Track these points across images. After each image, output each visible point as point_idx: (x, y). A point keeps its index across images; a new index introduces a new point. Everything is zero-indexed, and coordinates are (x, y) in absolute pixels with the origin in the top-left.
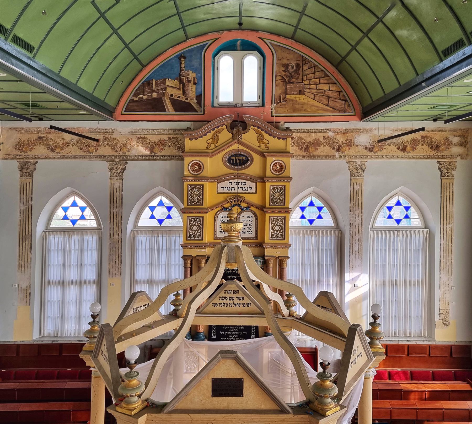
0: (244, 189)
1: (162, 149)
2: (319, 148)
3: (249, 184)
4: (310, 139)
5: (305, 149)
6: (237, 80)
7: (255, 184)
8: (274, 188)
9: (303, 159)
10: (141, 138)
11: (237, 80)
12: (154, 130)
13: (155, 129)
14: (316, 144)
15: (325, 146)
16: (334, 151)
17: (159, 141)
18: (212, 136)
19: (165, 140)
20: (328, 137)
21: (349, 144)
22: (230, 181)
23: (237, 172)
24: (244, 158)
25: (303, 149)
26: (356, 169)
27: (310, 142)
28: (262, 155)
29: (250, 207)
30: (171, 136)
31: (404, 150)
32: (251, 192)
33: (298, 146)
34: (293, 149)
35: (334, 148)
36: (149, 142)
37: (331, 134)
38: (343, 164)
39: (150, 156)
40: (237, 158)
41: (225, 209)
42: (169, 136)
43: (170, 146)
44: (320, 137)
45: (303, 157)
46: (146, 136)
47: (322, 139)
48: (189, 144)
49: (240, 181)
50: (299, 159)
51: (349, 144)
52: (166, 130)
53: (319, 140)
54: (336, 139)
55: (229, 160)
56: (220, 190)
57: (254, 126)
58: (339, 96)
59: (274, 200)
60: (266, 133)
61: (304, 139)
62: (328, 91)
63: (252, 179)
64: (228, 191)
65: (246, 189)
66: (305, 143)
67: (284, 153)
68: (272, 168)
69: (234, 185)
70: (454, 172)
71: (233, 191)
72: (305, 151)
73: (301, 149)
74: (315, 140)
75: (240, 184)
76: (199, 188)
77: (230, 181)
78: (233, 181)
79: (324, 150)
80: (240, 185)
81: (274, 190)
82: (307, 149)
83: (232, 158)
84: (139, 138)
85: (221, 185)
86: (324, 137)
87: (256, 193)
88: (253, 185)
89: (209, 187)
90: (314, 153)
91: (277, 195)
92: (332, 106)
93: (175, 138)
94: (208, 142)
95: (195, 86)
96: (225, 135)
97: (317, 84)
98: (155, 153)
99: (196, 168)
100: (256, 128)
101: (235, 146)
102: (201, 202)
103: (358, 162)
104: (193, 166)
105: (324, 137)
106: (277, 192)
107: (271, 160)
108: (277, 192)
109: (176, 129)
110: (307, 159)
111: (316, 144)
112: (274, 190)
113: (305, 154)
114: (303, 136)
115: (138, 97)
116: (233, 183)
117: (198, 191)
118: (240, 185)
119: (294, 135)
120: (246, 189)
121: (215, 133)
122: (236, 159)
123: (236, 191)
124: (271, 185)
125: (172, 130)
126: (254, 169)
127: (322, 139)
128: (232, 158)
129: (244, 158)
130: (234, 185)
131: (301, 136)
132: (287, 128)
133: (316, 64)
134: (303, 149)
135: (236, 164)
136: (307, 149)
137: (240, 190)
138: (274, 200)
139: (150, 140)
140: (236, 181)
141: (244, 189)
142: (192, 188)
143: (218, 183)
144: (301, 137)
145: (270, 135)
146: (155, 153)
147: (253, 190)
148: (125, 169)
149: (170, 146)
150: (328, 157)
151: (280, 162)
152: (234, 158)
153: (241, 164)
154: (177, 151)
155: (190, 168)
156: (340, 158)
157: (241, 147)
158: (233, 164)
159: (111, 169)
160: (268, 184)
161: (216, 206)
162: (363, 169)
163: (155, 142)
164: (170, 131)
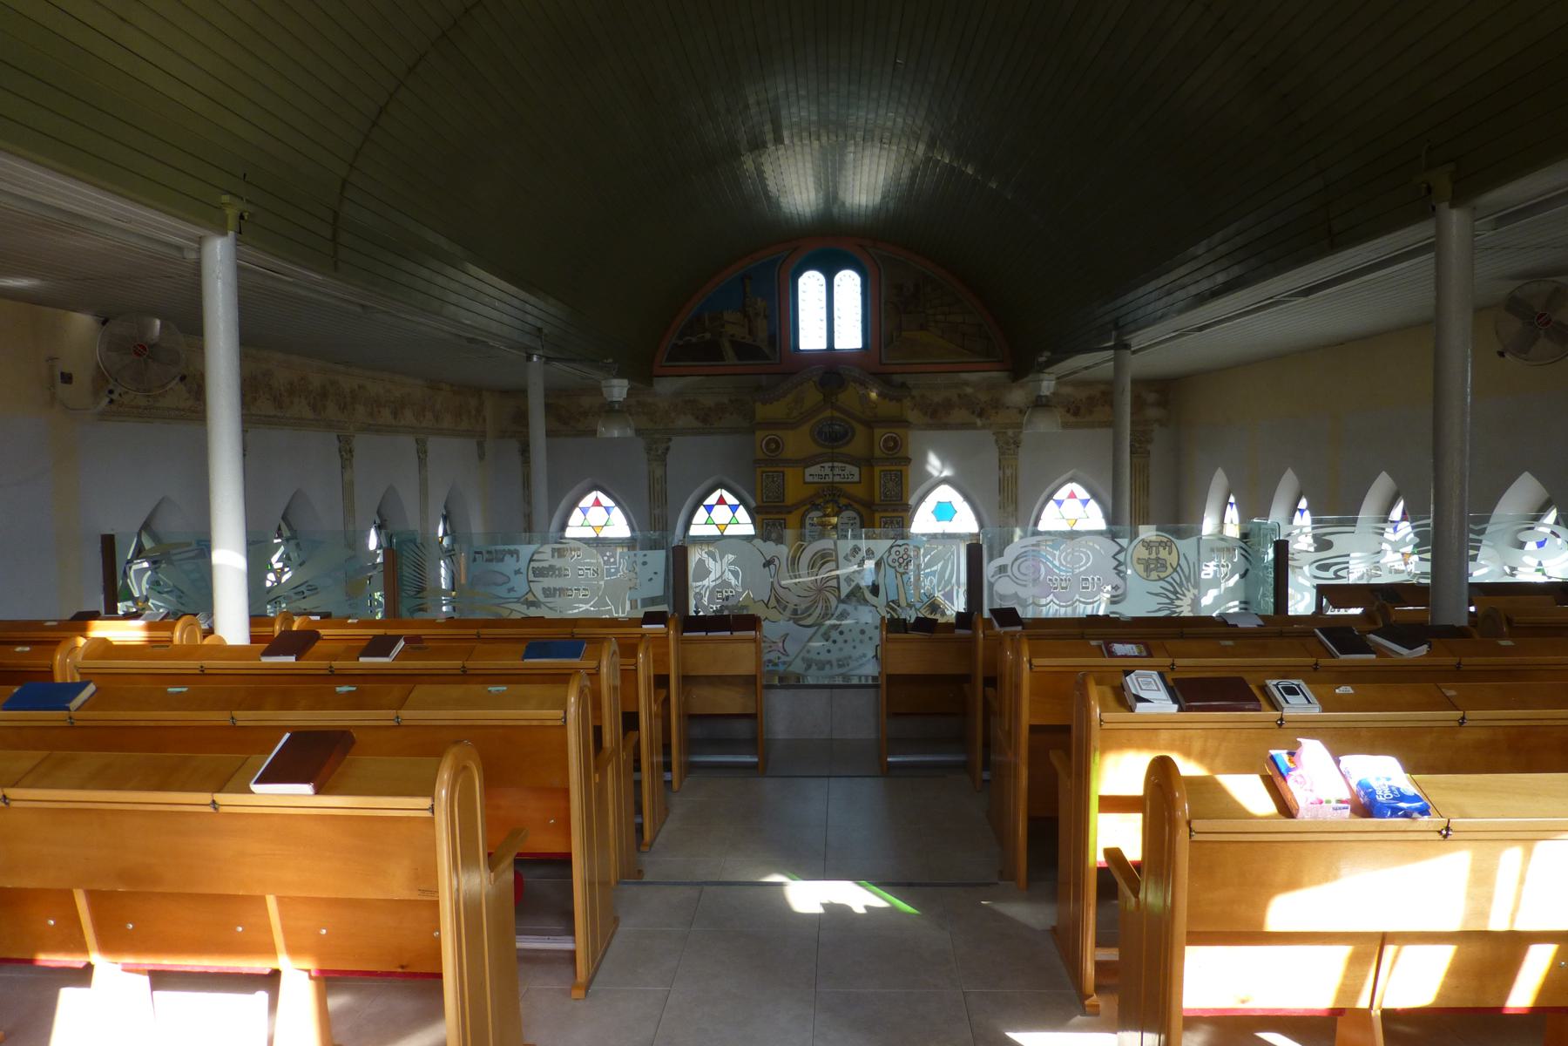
3: (849, 468)
6: (830, 312)
11: (830, 312)
14: (948, 406)
21: (997, 405)
26: (1007, 443)
28: (870, 424)
31: (1076, 413)
34: (913, 416)
37: (969, 390)
38: (988, 436)
41: (815, 507)
45: (929, 427)
48: (763, 411)
51: (997, 405)
56: (809, 479)
63: (853, 461)
67: (903, 423)
69: (828, 471)
70: (1150, 447)
78: (827, 465)
79: (959, 415)
80: (837, 471)
85: (808, 471)
88: (855, 470)
89: (790, 473)
96: (813, 396)
99: (773, 446)
101: (828, 413)
103: (1010, 432)
104: (768, 444)
107: (881, 434)
119: (915, 393)
126: (857, 446)
132: (903, 385)
137: (837, 479)
147: (856, 479)
148: (668, 449)
156: (983, 427)
157: (836, 414)
159: (649, 450)
160: (877, 470)
161: (802, 503)
162: (1017, 444)
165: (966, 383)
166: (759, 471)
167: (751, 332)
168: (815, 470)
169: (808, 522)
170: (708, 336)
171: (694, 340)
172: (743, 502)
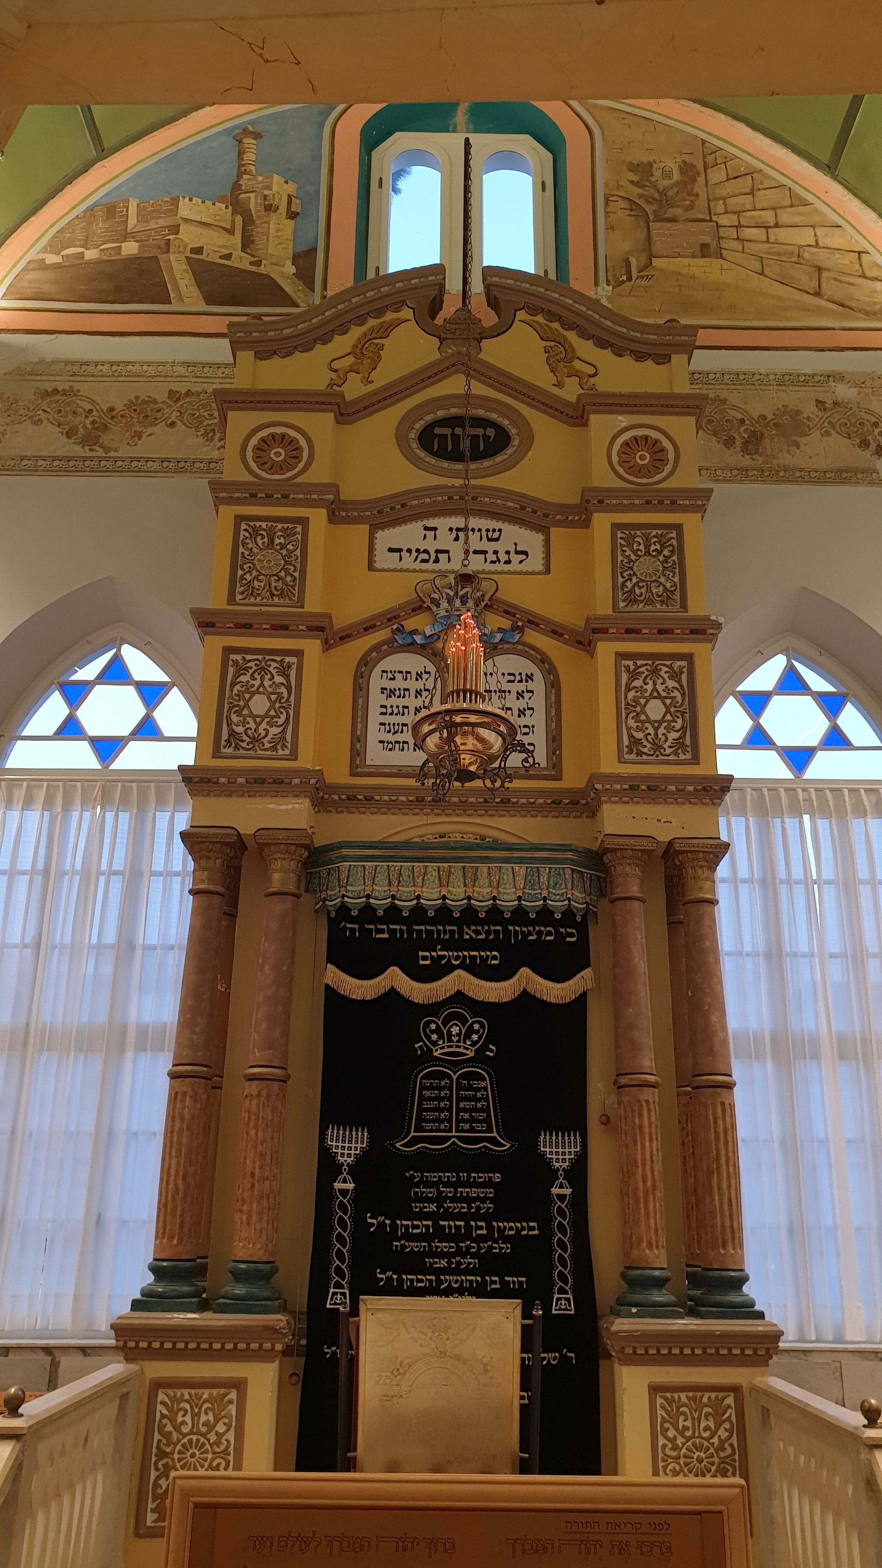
0: (491, 557)
1: (139, 435)
2: (802, 440)
3: (514, 535)
4: (761, 406)
5: (746, 443)
7: (540, 537)
8: (629, 541)
9: (741, 481)
10: (56, 391)
12: (112, 364)
13: (118, 363)
14: (791, 426)
15: (828, 434)
16: (867, 454)
17: (130, 405)
18: (355, 346)
19: (154, 401)
20: (836, 404)
22: (430, 523)
23: (458, 482)
24: (491, 432)
25: (738, 443)
27: (764, 417)
29: (521, 630)
30: (182, 388)
32: (523, 567)
33: (715, 434)
35: (864, 444)
36: (88, 406)
37: (844, 392)
39: (84, 459)
40: (458, 431)
42: (175, 387)
43: (173, 424)
44: (803, 401)
45: (743, 474)
46: (76, 386)
47: (810, 410)
49: (475, 522)
50: (726, 481)
52: (163, 364)
53: (798, 412)
54: (870, 412)
55: (426, 438)
57: (534, 311)
58: (857, 267)
59: (632, 591)
60: (584, 335)
61: (735, 408)
62: (815, 250)
64: (418, 565)
65: (503, 557)
66: (742, 421)
68: (615, 459)
69: (445, 540)
71: (443, 565)
72: (745, 450)
73: (729, 443)
74: (784, 410)
75: (474, 538)
76: (289, 534)
77: (430, 523)
78: (443, 523)
79: (823, 449)
81: (630, 545)
82: (753, 442)
83: (437, 431)
84: (46, 394)
85: (386, 538)
86: (820, 403)
87: (548, 570)
88: (532, 541)
90: (786, 459)
91: (645, 566)
92: (836, 298)
93: (198, 394)
94: (336, 365)
95: (291, 223)
97: (767, 228)
98: (107, 450)
100: (540, 319)
101: (455, 385)
102: (293, 588)
105: (820, 403)
106: (647, 553)
108: (647, 553)
109: (204, 365)
110: (756, 481)
111: (791, 426)
112: (630, 545)
113: (747, 461)
114: (734, 398)
115: (65, 253)
116: (443, 532)
117: (283, 546)
118: (475, 542)
120: (503, 557)
121: (367, 338)
122: (456, 438)
123: (456, 565)
124: (616, 527)
125: (187, 364)
127: (810, 410)
128: (437, 431)
129: (491, 432)
130: (445, 540)
131: (724, 395)
133: (760, 166)
134: (738, 443)
135: (456, 456)
136: (753, 442)
137: (476, 564)
138: (632, 591)
139: (92, 402)
140: (458, 522)
141: (491, 557)
142: (255, 533)
143: (375, 528)
144: (724, 401)
145: (602, 344)
146: (107, 450)
147: (535, 562)
149: (173, 424)
150: (842, 476)
151: (654, 434)
152: (447, 431)
153: (477, 456)
154: (201, 440)
155: (249, 454)
157: (479, 389)
158: (441, 454)
163: (112, 409)
164: (182, 370)
165: (839, 378)
166: (229, 512)
167: (247, 243)
168: (408, 535)
169: (376, 682)
170: (130, 248)
171: (91, 254)
172: (180, 678)
